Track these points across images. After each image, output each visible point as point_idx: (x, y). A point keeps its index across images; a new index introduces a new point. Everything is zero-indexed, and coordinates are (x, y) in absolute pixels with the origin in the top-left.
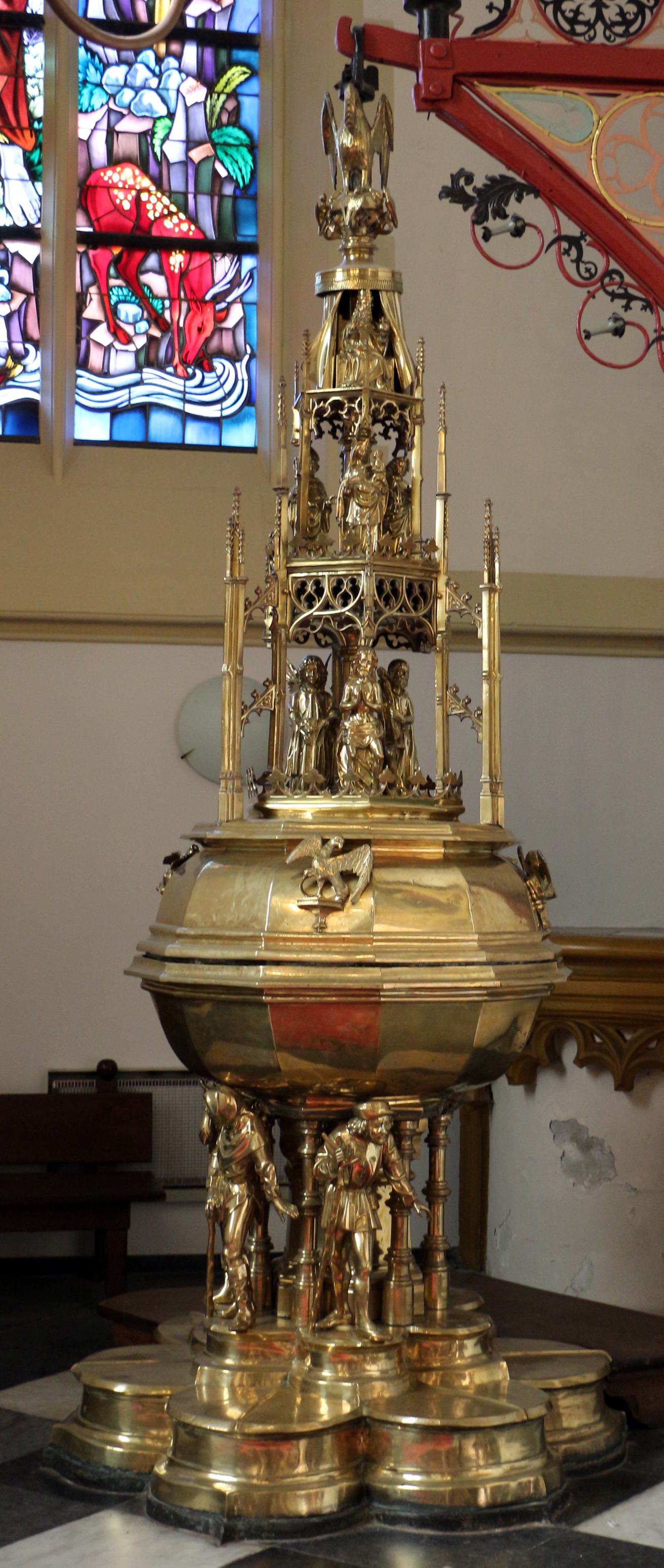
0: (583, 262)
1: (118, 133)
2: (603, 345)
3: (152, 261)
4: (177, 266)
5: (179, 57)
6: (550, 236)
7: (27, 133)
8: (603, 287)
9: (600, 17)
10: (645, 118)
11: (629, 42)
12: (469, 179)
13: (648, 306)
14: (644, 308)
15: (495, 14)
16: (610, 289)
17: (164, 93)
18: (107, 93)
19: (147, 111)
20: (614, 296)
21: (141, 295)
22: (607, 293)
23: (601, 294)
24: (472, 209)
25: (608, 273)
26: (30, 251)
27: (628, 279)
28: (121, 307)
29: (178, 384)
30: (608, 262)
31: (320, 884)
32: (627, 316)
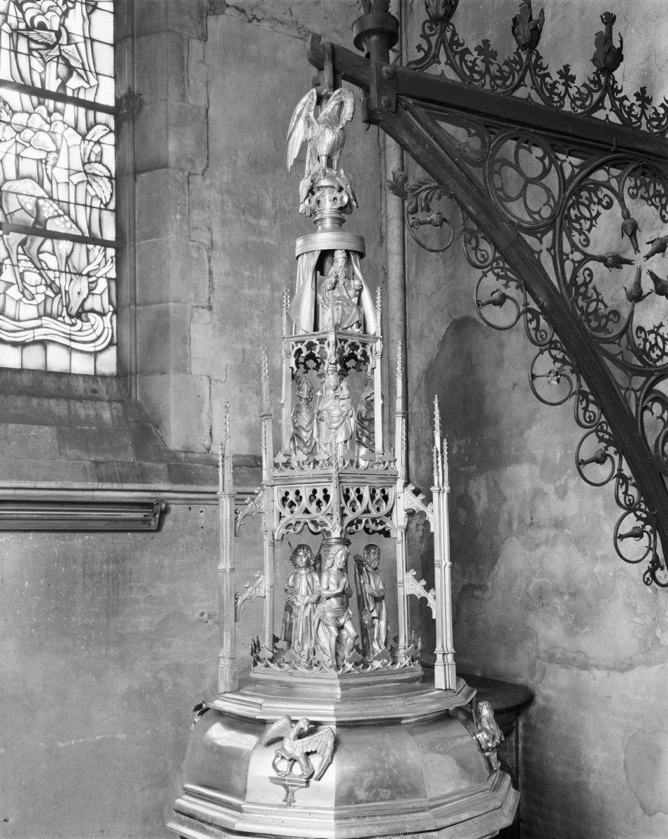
0: (480, 249)
1: (22, 157)
4: (64, 251)
14: (517, 288)
15: (422, 54)
16: (496, 271)
18: (15, 131)
19: (42, 146)
20: (498, 276)
21: (41, 269)
23: (490, 274)
28: (25, 273)
29: (67, 329)
32: (507, 292)
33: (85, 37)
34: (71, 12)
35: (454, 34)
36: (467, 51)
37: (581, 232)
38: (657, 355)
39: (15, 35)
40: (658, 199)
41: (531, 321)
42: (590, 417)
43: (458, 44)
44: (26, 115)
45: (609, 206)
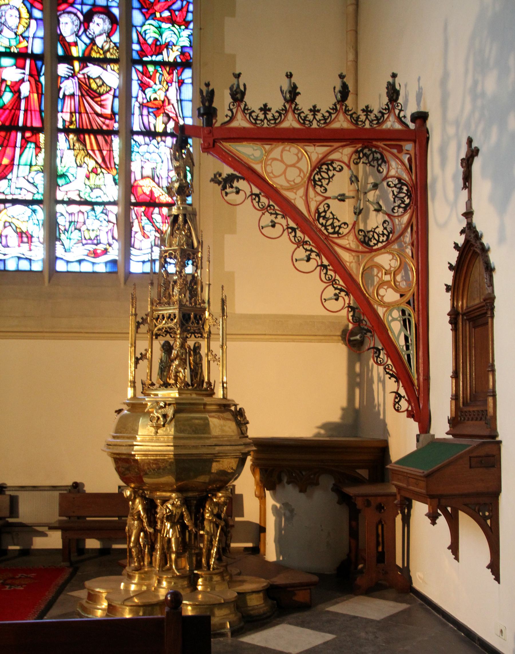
2: (269, 231)
3: (157, 210)
5: (165, 142)
6: (248, 193)
7: (114, 170)
8: (267, 211)
9: (265, 118)
10: (282, 152)
11: (276, 126)
12: (220, 175)
13: (283, 217)
14: (282, 218)
15: (228, 118)
16: (270, 211)
17: (160, 154)
20: (271, 214)
22: (269, 213)
23: (267, 214)
24: (221, 186)
25: (269, 206)
26: (114, 209)
27: (276, 207)
30: (269, 202)
31: (157, 418)
32: (276, 221)
33: (177, 100)
34: (170, 88)
35: (246, 105)
36: (253, 111)
37: (321, 186)
38: (374, 243)
39: (141, 107)
40: (375, 162)
41: (291, 233)
42: (329, 278)
43: (248, 109)
44: (146, 146)
45: (341, 170)
